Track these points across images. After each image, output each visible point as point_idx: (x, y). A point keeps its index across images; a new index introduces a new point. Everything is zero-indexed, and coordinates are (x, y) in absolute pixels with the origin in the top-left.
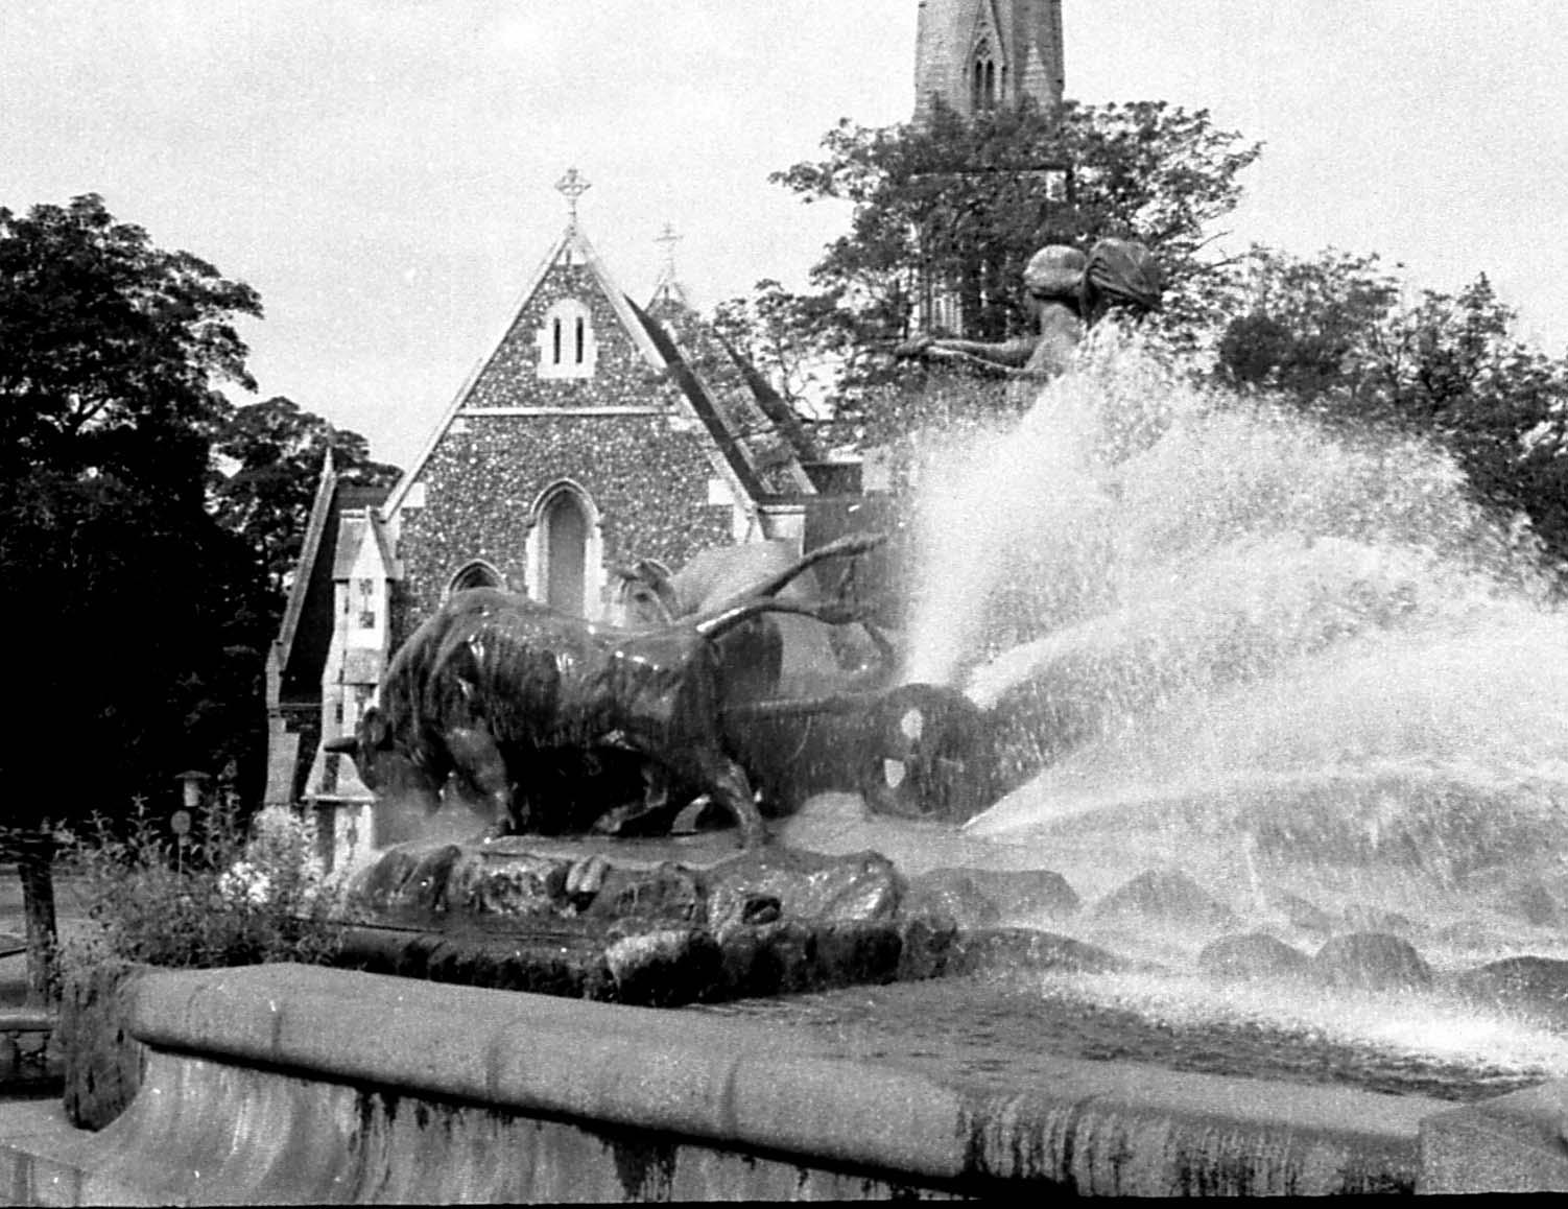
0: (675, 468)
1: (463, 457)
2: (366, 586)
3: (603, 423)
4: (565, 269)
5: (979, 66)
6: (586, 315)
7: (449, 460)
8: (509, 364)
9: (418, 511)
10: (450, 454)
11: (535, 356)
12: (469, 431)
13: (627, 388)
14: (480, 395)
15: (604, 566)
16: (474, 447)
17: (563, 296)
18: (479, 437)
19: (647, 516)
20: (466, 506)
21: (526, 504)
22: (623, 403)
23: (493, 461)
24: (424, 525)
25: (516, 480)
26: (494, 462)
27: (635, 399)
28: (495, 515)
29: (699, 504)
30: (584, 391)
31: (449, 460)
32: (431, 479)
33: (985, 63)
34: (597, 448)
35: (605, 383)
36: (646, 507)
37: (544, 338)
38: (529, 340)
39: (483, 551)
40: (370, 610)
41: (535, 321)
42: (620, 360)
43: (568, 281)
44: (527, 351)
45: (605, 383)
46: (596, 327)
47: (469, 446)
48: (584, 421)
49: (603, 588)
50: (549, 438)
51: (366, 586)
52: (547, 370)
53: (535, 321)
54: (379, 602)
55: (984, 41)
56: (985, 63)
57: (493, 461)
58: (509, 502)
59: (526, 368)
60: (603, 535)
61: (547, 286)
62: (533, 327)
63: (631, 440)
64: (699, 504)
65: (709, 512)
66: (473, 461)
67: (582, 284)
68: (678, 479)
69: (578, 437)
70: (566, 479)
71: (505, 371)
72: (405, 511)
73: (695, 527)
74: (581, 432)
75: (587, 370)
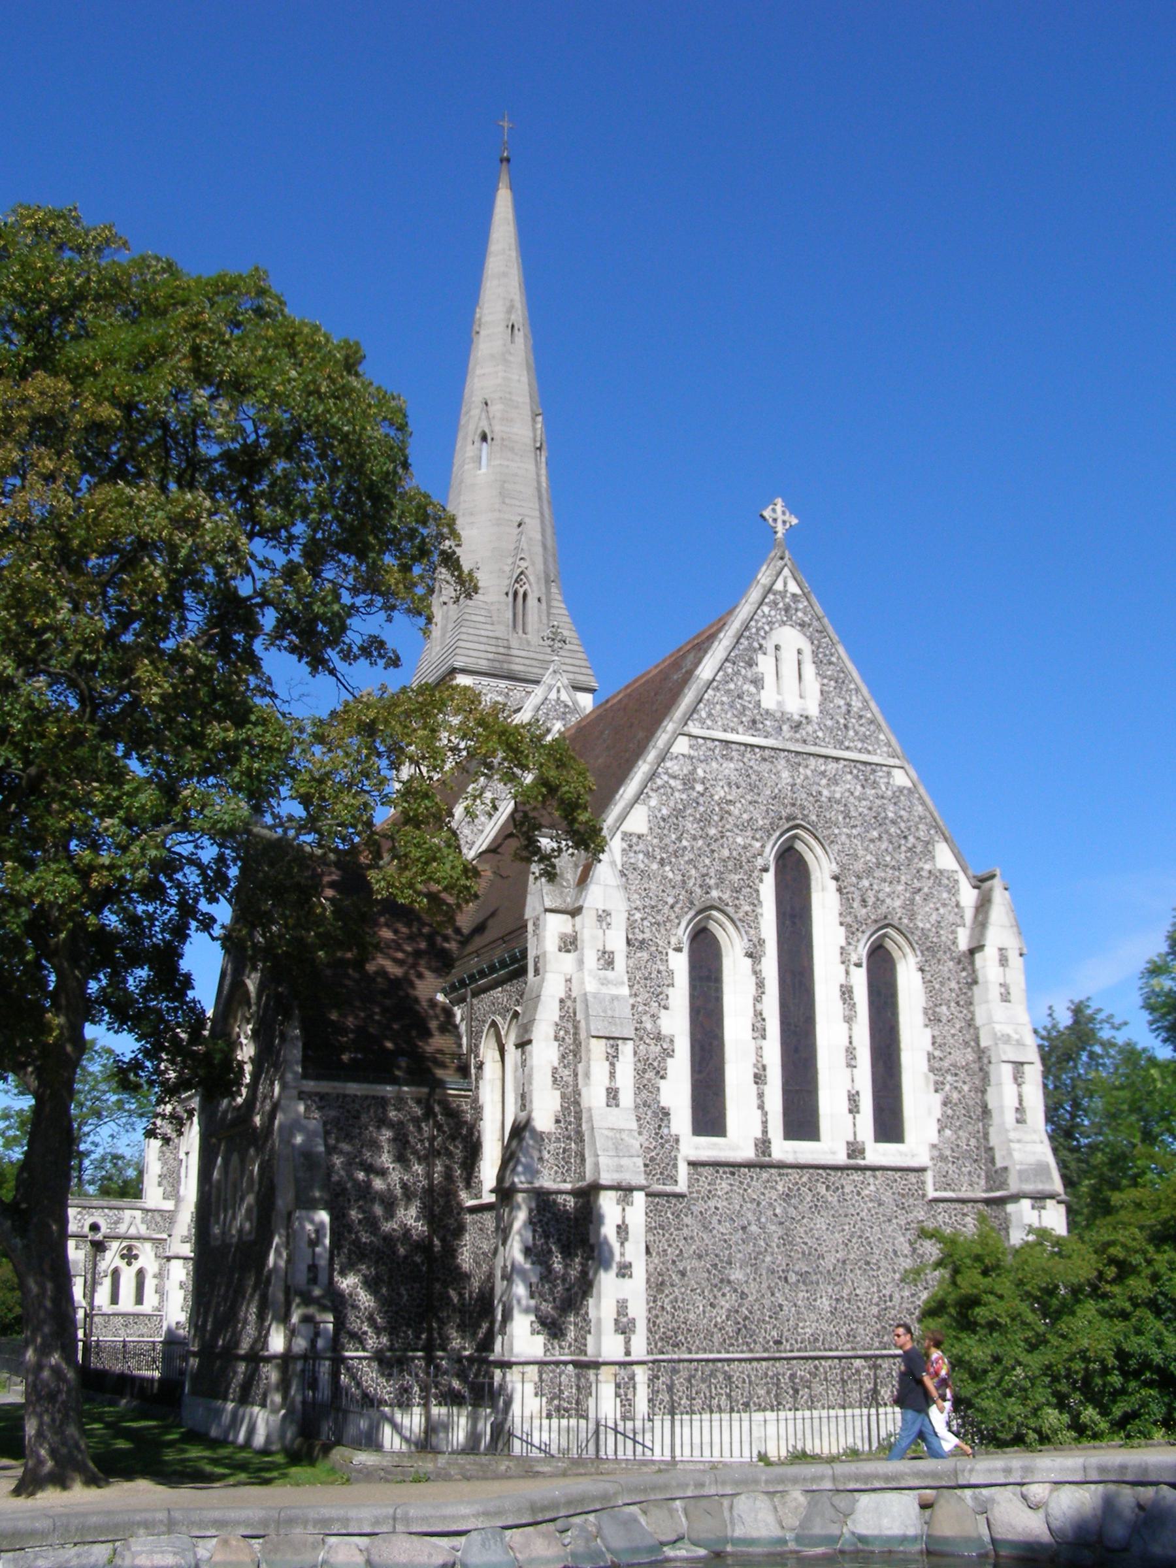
0: (903, 825)
1: (688, 782)
2: (603, 917)
3: (832, 767)
4: (783, 594)
5: (516, 594)
6: (807, 649)
7: (672, 782)
8: (732, 686)
9: (639, 837)
10: (675, 777)
11: (758, 682)
12: (692, 753)
13: (851, 733)
14: (704, 714)
15: (841, 924)
16: (700, 772)
17: (784, 623)
18: (705, 761)
19: (879, 873)
20: (695, 838)
21: (758, 845)
22: (848, 748)
23: (719, 793)
24: (647, 854)
25: (745, 816)
26: (722, 794)
27: (859, 745)
28: (726, 853)
29: (927, 867)
30: (810, 729)
31: (672, 782)
32: (653, 802)
33: (521, 591)
34: (826, 793)
35: (829, 723)
36: (878, 865)
37: (765, 664)
38: (751, 663)
39: (715, 894)
40: (608, 949)
41: (756, 645)
42: (842, 702)
43: (787, 609)
44: (749, 675)
45: (829, 723)
46: (818, 663)
47: (695, 769)
48: (812, 762)
49: (842, 948)
50: (777, 774)
51: (603, 917)
52: (769, 699)
53: (756, 645)
54: (616, 941)
55: (522, 573)
56: (521, 591)
57: (719, 793)
58: (739, 840)
59: (751, 695)
60: (839, 890)
61: (766, 609)
62: (755, 650)
63: (859, 787)
64: (927, 867)
65: (937, 876)
66: (699, 788)
67: (800, 614)
68: (905, 837)
69: (807, 778)
70: (798, 822)
71: (728, 692)
72: (626, 836)
73: (926, 890)
74: (809, 773)
75: (813, 711)
